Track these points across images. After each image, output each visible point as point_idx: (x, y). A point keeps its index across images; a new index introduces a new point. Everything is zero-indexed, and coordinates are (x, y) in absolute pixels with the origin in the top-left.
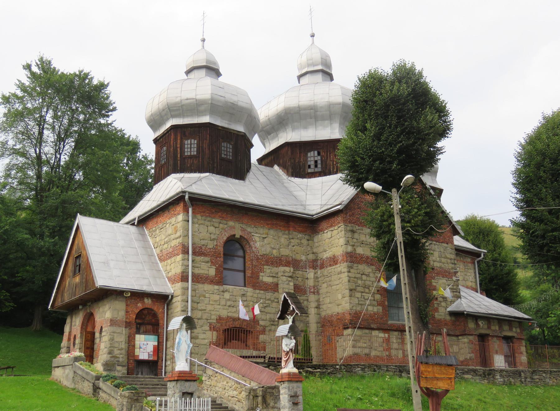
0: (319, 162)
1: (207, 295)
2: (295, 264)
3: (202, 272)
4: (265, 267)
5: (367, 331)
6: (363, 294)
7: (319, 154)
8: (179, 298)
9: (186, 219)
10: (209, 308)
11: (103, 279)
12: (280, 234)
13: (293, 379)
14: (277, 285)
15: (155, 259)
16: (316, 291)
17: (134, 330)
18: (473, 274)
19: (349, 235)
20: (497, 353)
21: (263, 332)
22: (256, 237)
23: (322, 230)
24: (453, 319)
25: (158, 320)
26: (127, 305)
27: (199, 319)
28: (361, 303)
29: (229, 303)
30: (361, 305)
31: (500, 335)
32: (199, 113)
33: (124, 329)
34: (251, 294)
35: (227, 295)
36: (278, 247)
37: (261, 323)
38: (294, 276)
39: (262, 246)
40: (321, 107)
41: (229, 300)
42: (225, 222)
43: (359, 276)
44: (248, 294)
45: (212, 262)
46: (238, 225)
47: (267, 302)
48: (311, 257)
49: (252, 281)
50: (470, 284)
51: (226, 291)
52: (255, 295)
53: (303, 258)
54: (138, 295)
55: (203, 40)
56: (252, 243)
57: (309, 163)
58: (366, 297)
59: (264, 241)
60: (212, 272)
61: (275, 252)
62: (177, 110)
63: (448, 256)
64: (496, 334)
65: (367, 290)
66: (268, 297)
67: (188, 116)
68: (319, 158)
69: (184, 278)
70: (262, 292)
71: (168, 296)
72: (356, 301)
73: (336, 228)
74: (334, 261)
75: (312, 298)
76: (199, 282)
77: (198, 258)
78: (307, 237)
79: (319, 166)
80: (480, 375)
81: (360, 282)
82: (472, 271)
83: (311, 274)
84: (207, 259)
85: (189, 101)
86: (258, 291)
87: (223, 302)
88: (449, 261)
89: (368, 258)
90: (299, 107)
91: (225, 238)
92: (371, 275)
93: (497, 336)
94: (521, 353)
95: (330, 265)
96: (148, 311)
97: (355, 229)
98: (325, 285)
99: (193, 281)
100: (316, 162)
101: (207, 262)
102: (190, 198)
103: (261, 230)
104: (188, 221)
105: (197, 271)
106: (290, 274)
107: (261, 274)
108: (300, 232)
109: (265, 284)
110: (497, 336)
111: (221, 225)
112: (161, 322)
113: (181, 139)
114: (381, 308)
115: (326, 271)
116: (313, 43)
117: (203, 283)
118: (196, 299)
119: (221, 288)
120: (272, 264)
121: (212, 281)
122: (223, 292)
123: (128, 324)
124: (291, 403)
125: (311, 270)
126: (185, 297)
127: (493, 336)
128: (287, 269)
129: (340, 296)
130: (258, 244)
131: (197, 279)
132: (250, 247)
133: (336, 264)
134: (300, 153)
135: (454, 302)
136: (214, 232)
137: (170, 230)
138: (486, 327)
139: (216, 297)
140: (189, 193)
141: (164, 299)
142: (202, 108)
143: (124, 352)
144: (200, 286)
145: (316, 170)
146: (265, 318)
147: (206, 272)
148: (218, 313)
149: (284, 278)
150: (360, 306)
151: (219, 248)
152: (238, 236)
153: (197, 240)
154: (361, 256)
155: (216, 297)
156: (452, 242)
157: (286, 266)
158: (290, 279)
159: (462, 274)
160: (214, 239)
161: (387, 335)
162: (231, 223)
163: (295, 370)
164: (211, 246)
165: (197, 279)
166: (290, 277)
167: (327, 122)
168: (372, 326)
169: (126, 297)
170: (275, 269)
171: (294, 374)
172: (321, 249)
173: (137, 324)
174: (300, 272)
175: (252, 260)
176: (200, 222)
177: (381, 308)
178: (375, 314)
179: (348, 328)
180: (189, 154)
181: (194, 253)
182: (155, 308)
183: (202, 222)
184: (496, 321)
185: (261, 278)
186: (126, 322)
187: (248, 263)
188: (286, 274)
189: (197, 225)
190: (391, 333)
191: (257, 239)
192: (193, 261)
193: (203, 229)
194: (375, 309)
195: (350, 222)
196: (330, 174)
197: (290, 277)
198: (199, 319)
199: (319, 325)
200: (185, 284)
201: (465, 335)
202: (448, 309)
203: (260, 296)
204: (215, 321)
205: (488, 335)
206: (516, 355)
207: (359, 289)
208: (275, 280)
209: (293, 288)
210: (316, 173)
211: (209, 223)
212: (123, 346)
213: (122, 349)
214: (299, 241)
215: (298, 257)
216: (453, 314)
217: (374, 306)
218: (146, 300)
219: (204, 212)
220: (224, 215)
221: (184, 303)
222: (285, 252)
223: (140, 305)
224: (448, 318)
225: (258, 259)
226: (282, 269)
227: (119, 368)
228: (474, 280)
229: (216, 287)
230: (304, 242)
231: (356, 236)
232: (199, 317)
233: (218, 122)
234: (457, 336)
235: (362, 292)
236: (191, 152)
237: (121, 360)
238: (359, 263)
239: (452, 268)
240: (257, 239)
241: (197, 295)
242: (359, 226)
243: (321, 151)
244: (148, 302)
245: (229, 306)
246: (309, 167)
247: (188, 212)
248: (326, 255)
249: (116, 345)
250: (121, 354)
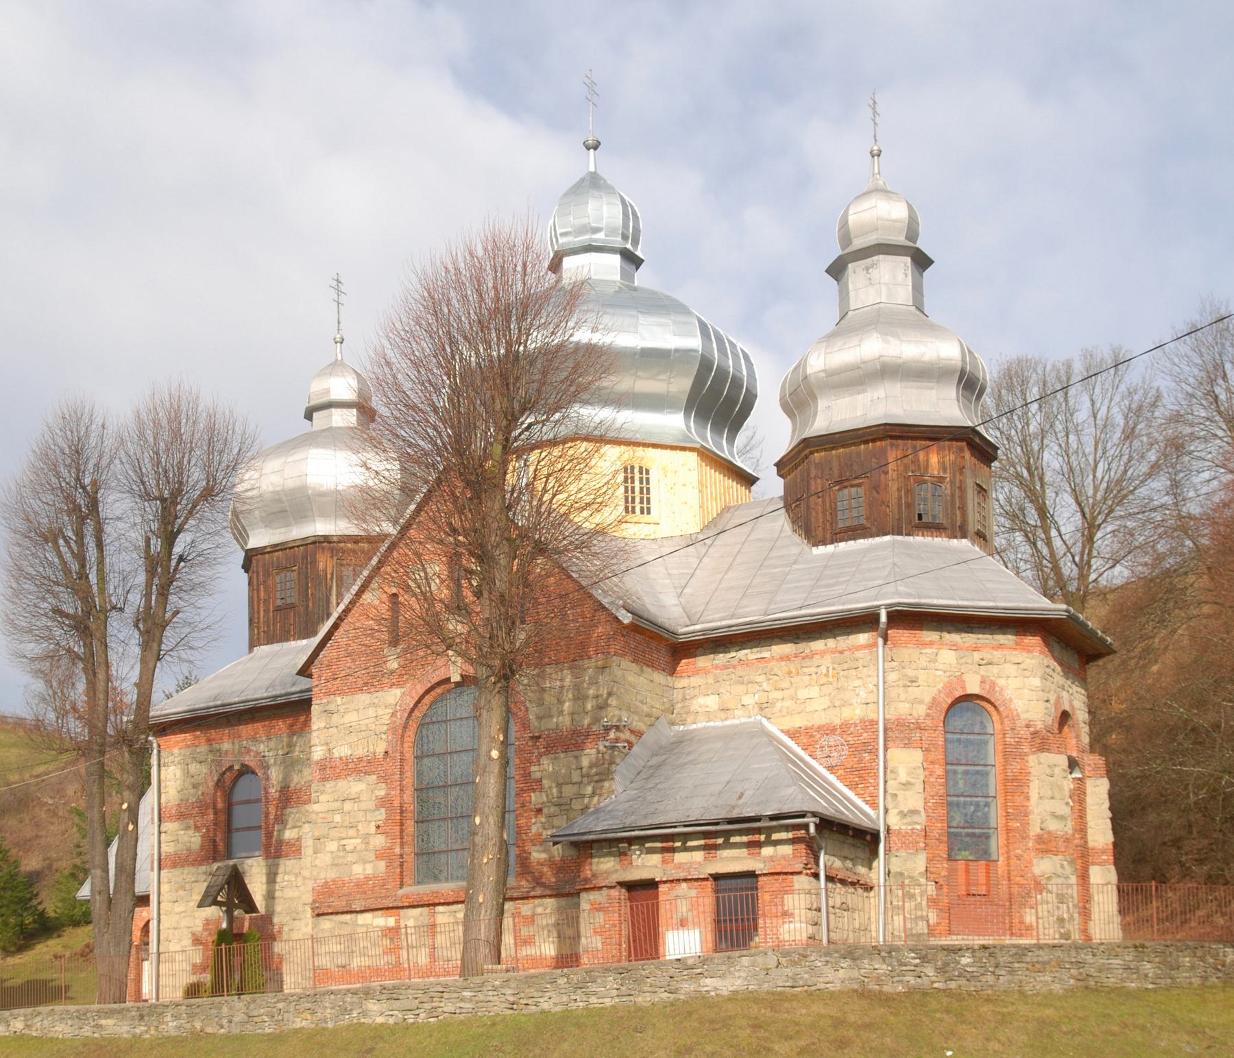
6: (343, 842)
20: (683, 924)
43: (337, 805)
65: (352, 832)
81: (337, 818)
89: (360, 760)
92: (363, 798)
93: (685, 880)
94: (786, 914)
110: (685, 880)
114: (382, 864)
154: (345, 761)
161: (391, 922)
177: (382, 864)
178: (367, 878)
190: (402, 912)
194: (369, 870)
207: (334, 833)
217: (365, 862)
231: (335, 719)
238: (338, 777)
242: (345, 694)
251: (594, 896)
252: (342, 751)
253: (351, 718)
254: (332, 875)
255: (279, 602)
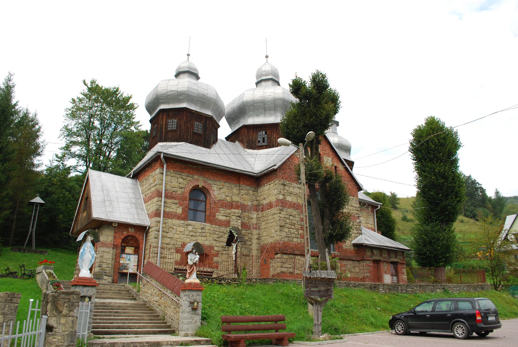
0: (266, 139)
1: (175, 227)
2: (243, 207)
3: (172, 210)
4: (220, 209)
5: (292, 256)
6: (290, 230)
7: (266, 133)
8: (153, 229)
9: (162, 172)
10: (176, 236)
11: (98, 213)
12: (233, 186)
13: (193, 288)
14: (229, 222)
15: (141, 202)
16: (257, 227)
17: (119, 250)
18: (373, 220)
19: (282, 187)
21: (217, 255)
22: (215, 188)
23: (264, 185)
24: (356, 249)
25: (139, 244)
26: (115, 233)
27: (167, 244)
28: (288, 235)
29: (191, 234)
30: (288, 237)
31: (388, 260)
32: (180, 101)
33: (112, 249)
34: (209, 228)
35: (190, 228)
36: (230, 195)
37: (216, 248)
38: (242, 216)
39: (219, 194)
40: (269, 101)
41: (192, 231)
42: (192, 176)
44: (207, 227)
45: (180, 204)
46: (201, 179)
47: (221, 234)
48: (255, 203)
49: (210, 219)
50: (370, 226)
51: (190, 225)
52: (212, 229)
53: (250, 204)
54: (123, 226)
55: (188, 55)
56: (211, 192)
57: (259, 139)
58: (292, 232)
59: (219, 191)
60: (180, 211)
61: (228, 198)
62: (164, 99)
63: (354, 205)
64: (386, 260)
65: (293, 227)
66: (221, 231)
67: (171, 103)
68: (266, 136)
69: (157, 214)
70: (217, 227)
71: (146, 227)
72: (285, 234)
73: (273, 182)
74: (270, 206)
75: (255, 232)
76: (169, 218)
77: (169, 201)
78: (253, 189)
79: (266, 141)
80: (368, 288)
81: (288, 221)
82: (372, 217)
83: (254, 215)
84: (176, 201)
85: (172, 92)
86: (214, 226)
87: (187, 233)
88: (354, 208)
89: (295, 204)
90: (253, 101)
91: (191, 187)
92: (297, 216)
93: (386, 262)
94: (403, 273)
95: (268, 209)
96: (131, 236)
97: (285, 183)
98: (264, 223)
99: (164, 216)
100: (264, 138)
101: (176, 204)
102: (164, 157)
103: (219, 183)
104: (163, 174)
105: (167, 210)
106: (239, 215)
107: (217, 214)
108: (248, 185)
109: (220, 221)
110: (386, 262)
111: (188, 178)
112: (141, 246)
113: (166, 119)
115: (264, 213)
116: (267, 62)
117: (172, 218)
118: (165, 230)
119: (186, 223)
120: (226, 207)
121: (179, 218)
122: (187, 225)
123: (115, 246)
124: (190, 308)
125: (255, 212)
126: (157, 228)
127: (384, 262)
128: (237, 211)
129: (273, 231)
130: (216, 193)
131: (167, 215)
132: (210, 194)
133: (272, 208)
134: (253, 132)
135: (357, 237)
136: (181, 183)
137: (151, 180)
138: (379, 255)
139: (182, 229)
140: (164, 153)
141: (143, 230)
142: (181, 97)
143: (110, 266)
144: (170, 220)
145: (264, 144)
146: (218, 245)
147: (175, 211)
148: (183, 241)
149: (234, 217)
150: (287, 238)
151: (186, 194)
152: (200, 186)
153: (169, 188)
155: (182, 229)
156: (357, 196)
157: (236, 209)
158: (238, 218)
159: (365, 219)
160: (182, 188)
162: (196, 177)
163: (197, 281)
164: (180, 192)
165: (167, 215)
166: (239, 216)
167: (273, 112)
168: (296, 253)
169: (115, 227)
170: (228, 211)
171: (196, 284)
172: (262, 198)
173: (122, 246)
174: (247, 214)
175: (211, 204)
176: (172, 175)
178: (298, 244)
179: (278, 254)
180: (171, 129)
181: (166, 197)
182: (137, 236)
183: (174, 175)
184: (386, 251)
185: (217, 216)
186: (114, 244)
187: (208, 206)
188: (236, 215)
189: (170, 177)
191: (215, 189)
192: (165, 202)
193: (174, 180)
195: (282, 178)
196: (273, 147)
197: (239, 216)
198: (167, 244)
199: (259, 251)
200: (157, 219)
201: (364, 260)
202: (353, 242)
203: (215, 229)
204: (180, 246)
205: (380, 261)
206: (400, 274)
207: (287, 226)
208: (228, 218)
209: (240, 224)
210: (264, 146)
211: (179, 176)
212: (110, 262)
213: (109, 264)
214: (246, 192)
215: (246, 203)
216: (355, 245)
217: (298, 238)
218: (130, 229)
219: (175, 168)
220: (191, 171)
221: (157, 233)
222: (236, 199)
223: (125, 233)
224: (352, 248)
225: (215, 203)
226: (233, 210)
227: (105, 277)
228: (373, 223)
229: (182, 222)
230: (251, 192)
232: (167, 242)
233: (193, 108)
234: (358, 261)
235: (289, 228)
236: (172, 127)
237: (107, 271)
239: (356, 214)
240: (215, 189)
241: (167, 227)
243: (268, 131)
244: (131, 231)
245: (191, 236)
246: (259, 142)
247: (163, 168)
248: (265, 202)
249: (105, 261)
250: (108, 267)
251: (368, 262)
252: (289, 198)
253: (291, 190)
254: (286, 240)
255: (195, 131)
